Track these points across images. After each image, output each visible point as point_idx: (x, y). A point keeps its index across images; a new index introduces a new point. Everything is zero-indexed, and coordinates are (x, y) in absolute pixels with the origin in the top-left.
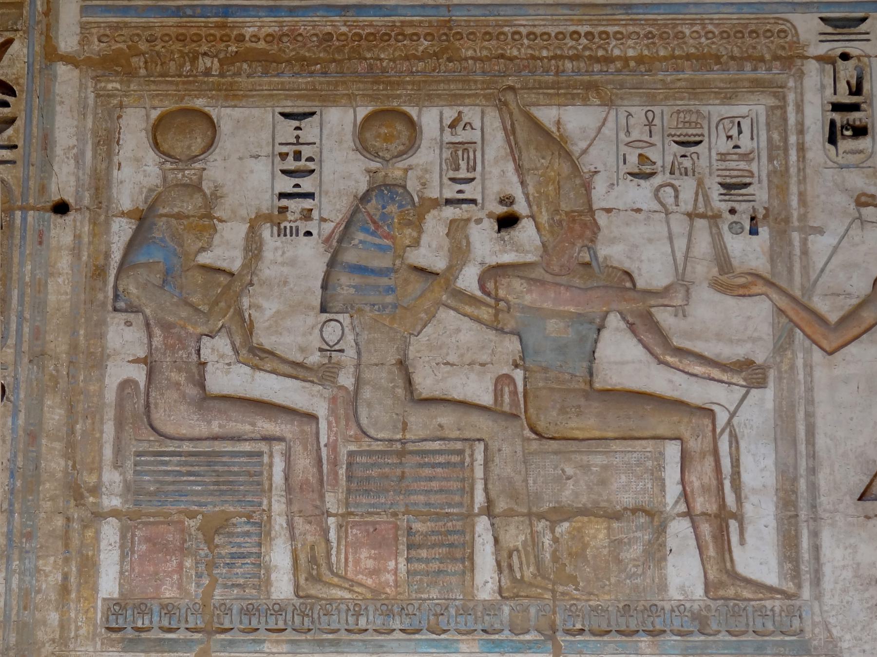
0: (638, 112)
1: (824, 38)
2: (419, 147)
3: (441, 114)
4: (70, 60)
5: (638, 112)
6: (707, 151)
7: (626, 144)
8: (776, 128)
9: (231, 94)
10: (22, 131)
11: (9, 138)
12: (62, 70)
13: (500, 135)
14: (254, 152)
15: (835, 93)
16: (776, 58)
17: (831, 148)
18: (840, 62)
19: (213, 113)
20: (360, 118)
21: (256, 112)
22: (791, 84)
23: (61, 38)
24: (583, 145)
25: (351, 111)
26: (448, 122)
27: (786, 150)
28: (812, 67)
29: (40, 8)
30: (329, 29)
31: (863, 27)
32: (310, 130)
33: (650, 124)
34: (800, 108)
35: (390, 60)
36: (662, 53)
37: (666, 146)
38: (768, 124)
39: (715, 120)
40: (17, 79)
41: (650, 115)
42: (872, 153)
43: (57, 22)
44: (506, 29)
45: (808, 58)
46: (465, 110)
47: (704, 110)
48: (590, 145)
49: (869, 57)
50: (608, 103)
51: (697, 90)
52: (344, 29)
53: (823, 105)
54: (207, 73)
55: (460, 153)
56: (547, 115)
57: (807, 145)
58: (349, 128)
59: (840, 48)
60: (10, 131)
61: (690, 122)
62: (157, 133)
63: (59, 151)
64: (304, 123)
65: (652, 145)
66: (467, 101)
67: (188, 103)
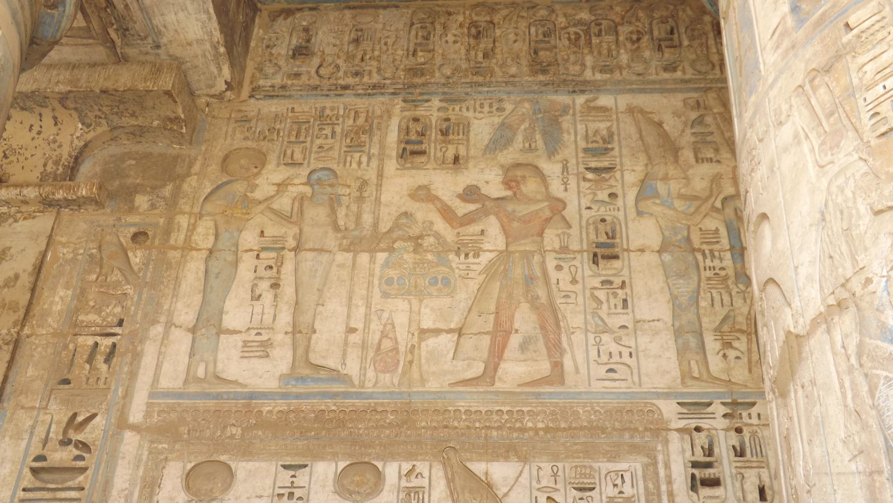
0: (546, 467)
1: (682, 416)
2: (382, 490)
3: (400, 466)
4: (135, 428)
5: (546, 467)
6: (599, 496)
7: (538, 489)
8: (651, 479)
9: (247, 452)
10: (90, 478)
11: (80, 482)
12: (128, 435)
13: (443, 483)
14: (259, 493)
15: (693, 454)
16: (646, 429)
17: (694, 495)
18: (695, 433)
19: (233, 465)
20: (339, 470)
21: (263, 465)
22: (659, 448)
23: (131, 414)
24: (505, 490)
25: (334, 464)
26: (404, 472)
27: (659, 495)
28: (674, 437)
29: (120, 394)
30: (323, 408)
31: (710, 409)
32: (302, 477)
33: (555, 475)
34: (667, 466)
35: (366, 429)
36: (563, 425)
37: (568, 491)
38: (644, 476)
39: (604, 472)
40: (94, 441)
41: (555, 469)
42: (726, 498)
43: (131, 403)
44: (450, 408)
45: (671, 430)
46: (418, 464)
47: (596, 465)
48: (509, 490)
49: (716, 430)
50: (524, 459)
51: (589, 452)
52: (334, 408)
53: (685, 464)
54: (232, 436)
55: (412, 495)
56: (478, 468)
57: (675, 492)
58: (331, 476)
59: (693, 423)
60: (81, 478)
61: (585, 474)
62: (189, 479)
63: (114, 492)
64: (299, 473)
65: (557, 490)
66: (419, 458)
67: (215, 457)
